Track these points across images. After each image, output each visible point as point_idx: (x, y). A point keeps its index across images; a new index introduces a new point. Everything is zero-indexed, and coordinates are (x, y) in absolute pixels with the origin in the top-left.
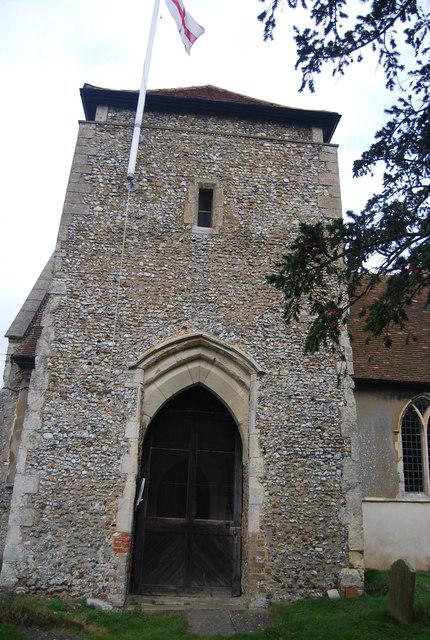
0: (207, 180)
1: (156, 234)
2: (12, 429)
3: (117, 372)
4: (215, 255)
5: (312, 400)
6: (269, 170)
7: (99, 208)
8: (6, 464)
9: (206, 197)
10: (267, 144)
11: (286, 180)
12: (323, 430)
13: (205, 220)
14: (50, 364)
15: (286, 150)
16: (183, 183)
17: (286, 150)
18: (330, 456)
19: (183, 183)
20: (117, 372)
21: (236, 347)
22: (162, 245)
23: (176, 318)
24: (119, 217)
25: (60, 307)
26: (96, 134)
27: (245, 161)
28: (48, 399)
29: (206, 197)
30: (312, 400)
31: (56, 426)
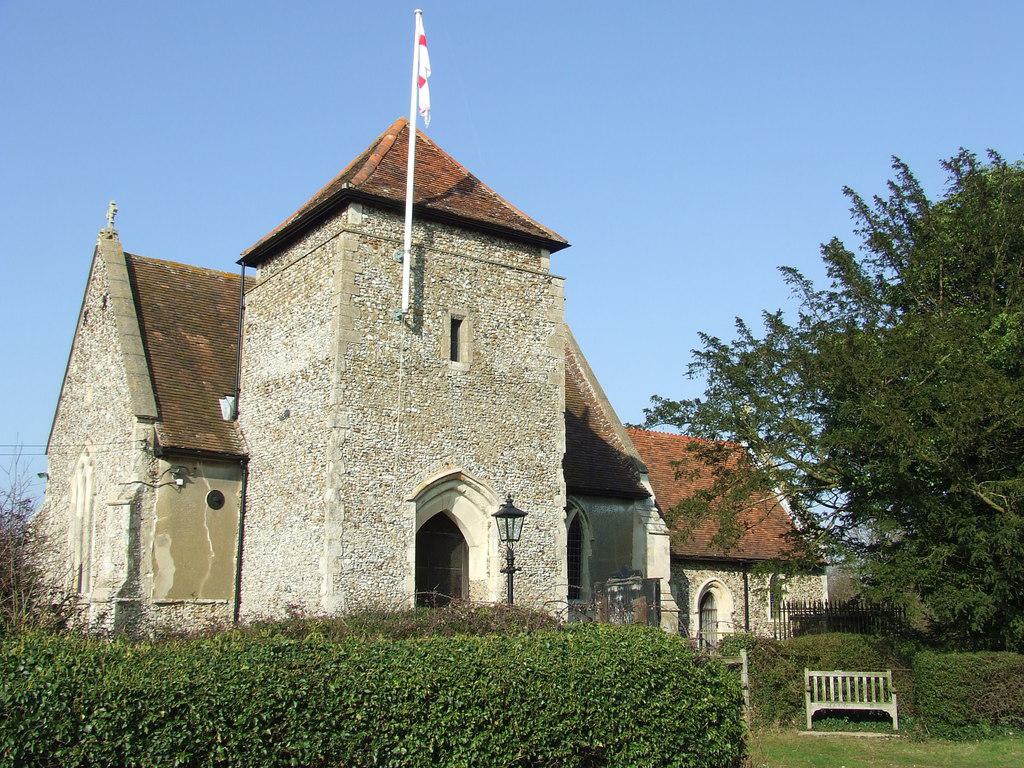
0: (458, 311)
1: (417, 368)
2: (152, 534)
3: (397, 504)
4: (467, 392)
5: (537, 528)
6: (509, 302)
7: (369, 337)
8: (149, 575)
9: (456, 324)
10: (508, 273)
11: (523, 315)
12: (543, 553)
13: (454, 357)
14: (343, 496)
15: (523, 280)
16: (439, 314)
17: (523, 280)
18: (547, 574)
19: (439, 314)
20: (397, 504)
21: (483, 482)
22: (425, 380)
23: (438, 452)
24: (387, 348)
25: (346, 441)
26: (359, 247)
27: (490, 291)
28: (345, 529)
29: (456, 324)
30: (537, 528)
31: (353, 552)
